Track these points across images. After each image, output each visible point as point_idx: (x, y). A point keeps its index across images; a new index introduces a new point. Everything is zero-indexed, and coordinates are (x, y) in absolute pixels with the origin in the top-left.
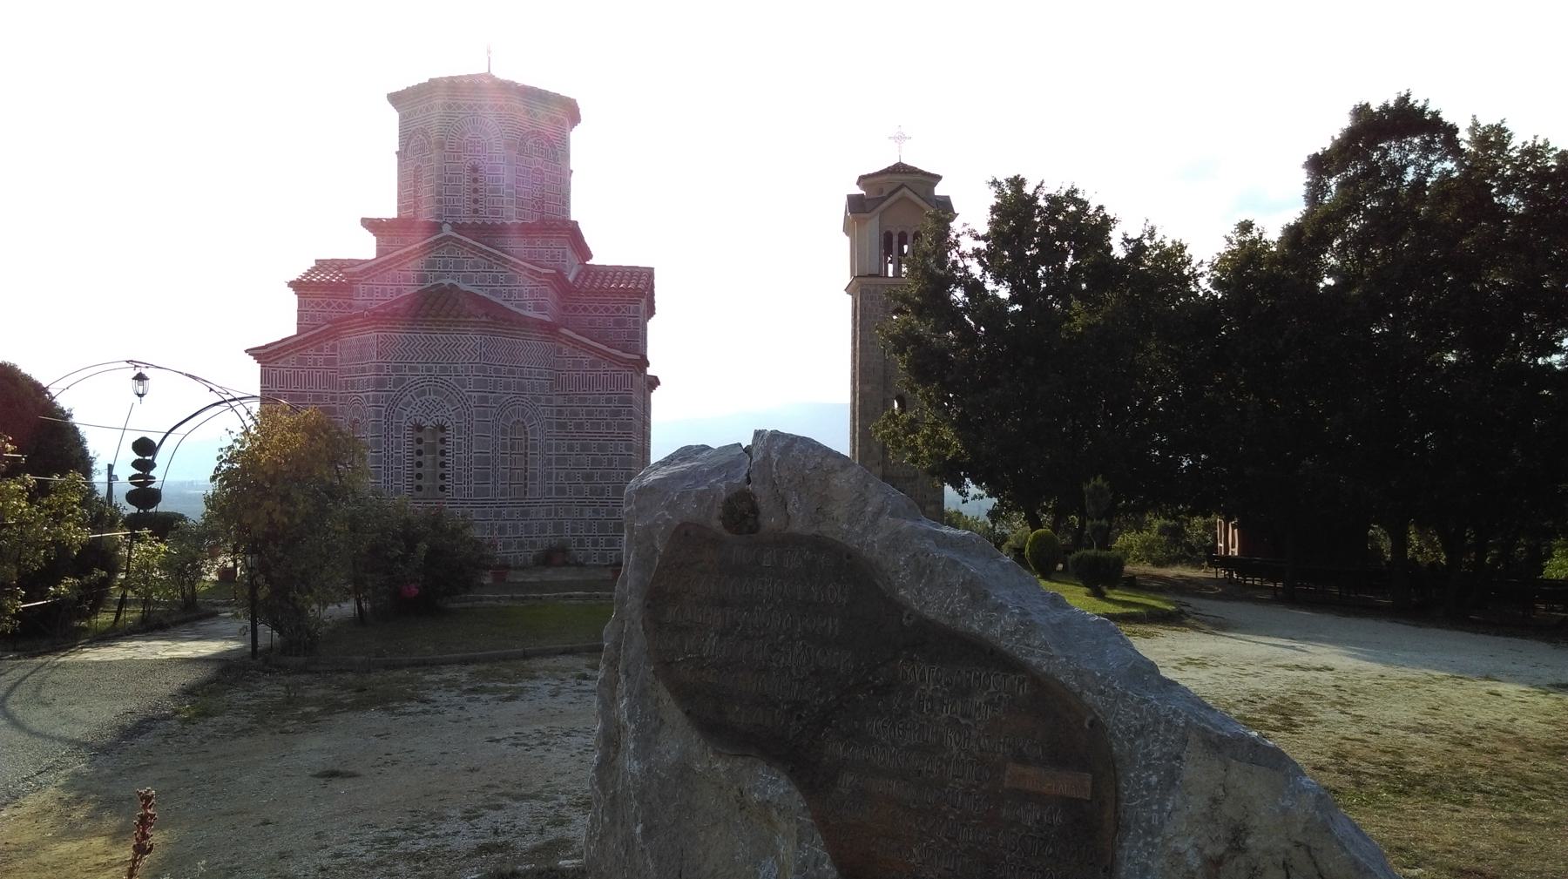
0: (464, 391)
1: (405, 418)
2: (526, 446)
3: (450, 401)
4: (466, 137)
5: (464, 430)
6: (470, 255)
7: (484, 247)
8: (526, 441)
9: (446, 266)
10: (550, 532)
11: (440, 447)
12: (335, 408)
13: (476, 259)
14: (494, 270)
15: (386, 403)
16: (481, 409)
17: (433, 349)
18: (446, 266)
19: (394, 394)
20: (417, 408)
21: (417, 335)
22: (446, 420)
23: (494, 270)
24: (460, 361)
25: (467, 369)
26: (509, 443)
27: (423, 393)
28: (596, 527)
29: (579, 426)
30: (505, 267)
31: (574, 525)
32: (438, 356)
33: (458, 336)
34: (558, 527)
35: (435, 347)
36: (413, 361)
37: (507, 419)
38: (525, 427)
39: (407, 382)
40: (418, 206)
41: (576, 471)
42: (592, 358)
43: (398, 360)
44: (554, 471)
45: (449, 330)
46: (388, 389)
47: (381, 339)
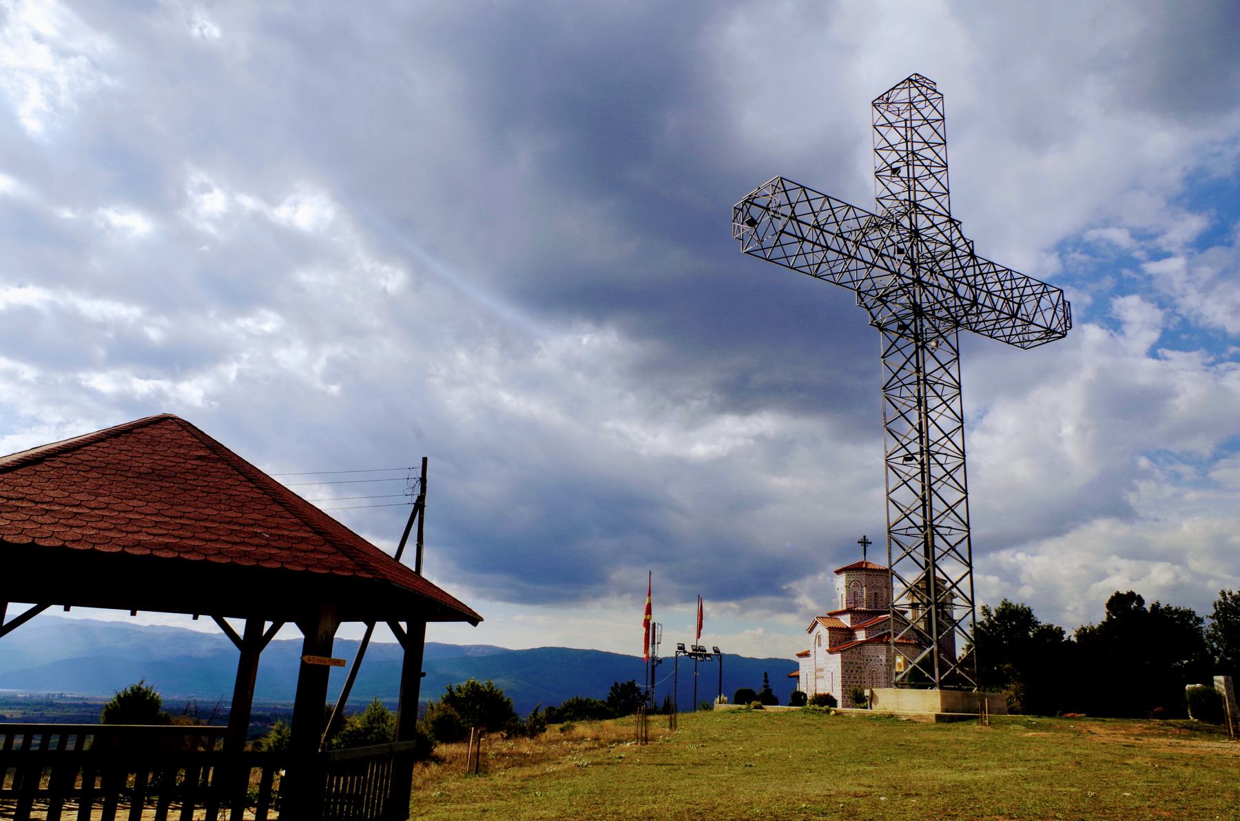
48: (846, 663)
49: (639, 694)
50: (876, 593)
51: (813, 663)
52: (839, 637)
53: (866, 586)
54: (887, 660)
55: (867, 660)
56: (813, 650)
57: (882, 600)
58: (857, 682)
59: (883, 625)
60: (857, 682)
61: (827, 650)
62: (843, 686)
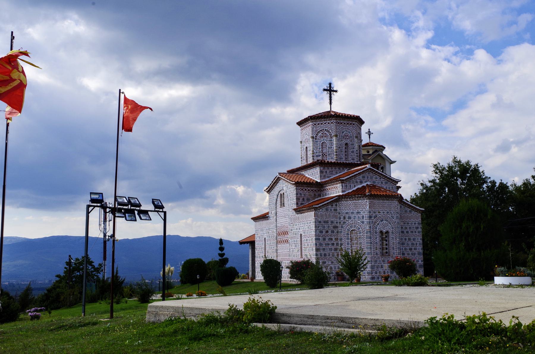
1: (378, 229)
3: (390, 223)
6: (374, 175)
9: (368, 178)
12: (337, 226)
13: (376, 176)
14: (381, 180)
15: (372, 223)
19: (374, 221)
20: (381, 226)
21: (380, 201)
23: (381, 180)
25: (394, 212)
27: (382, 221)
29: (407, 232)
30: (385, 179)
36: (379, 210)
39: (378, 217)
40: (323, 156)
42: (410, 209)
43: (375, 209)
44: (401, 247)
45: (389, 200)
46: (372, 219)
47: (370, 202)
48: (320, 222)
49: (93, 267)
50: (346, 144)
51: (273, 226)
52: (307, 193)
53: (336, 136)
54: (370, 217)
55: (344, 218)
56: (274, 212)
57: (353, 152)
58: (333, 244)
59: (361, 177)
60: (333, 244)
61: (295, 210)
62: (317, 250)
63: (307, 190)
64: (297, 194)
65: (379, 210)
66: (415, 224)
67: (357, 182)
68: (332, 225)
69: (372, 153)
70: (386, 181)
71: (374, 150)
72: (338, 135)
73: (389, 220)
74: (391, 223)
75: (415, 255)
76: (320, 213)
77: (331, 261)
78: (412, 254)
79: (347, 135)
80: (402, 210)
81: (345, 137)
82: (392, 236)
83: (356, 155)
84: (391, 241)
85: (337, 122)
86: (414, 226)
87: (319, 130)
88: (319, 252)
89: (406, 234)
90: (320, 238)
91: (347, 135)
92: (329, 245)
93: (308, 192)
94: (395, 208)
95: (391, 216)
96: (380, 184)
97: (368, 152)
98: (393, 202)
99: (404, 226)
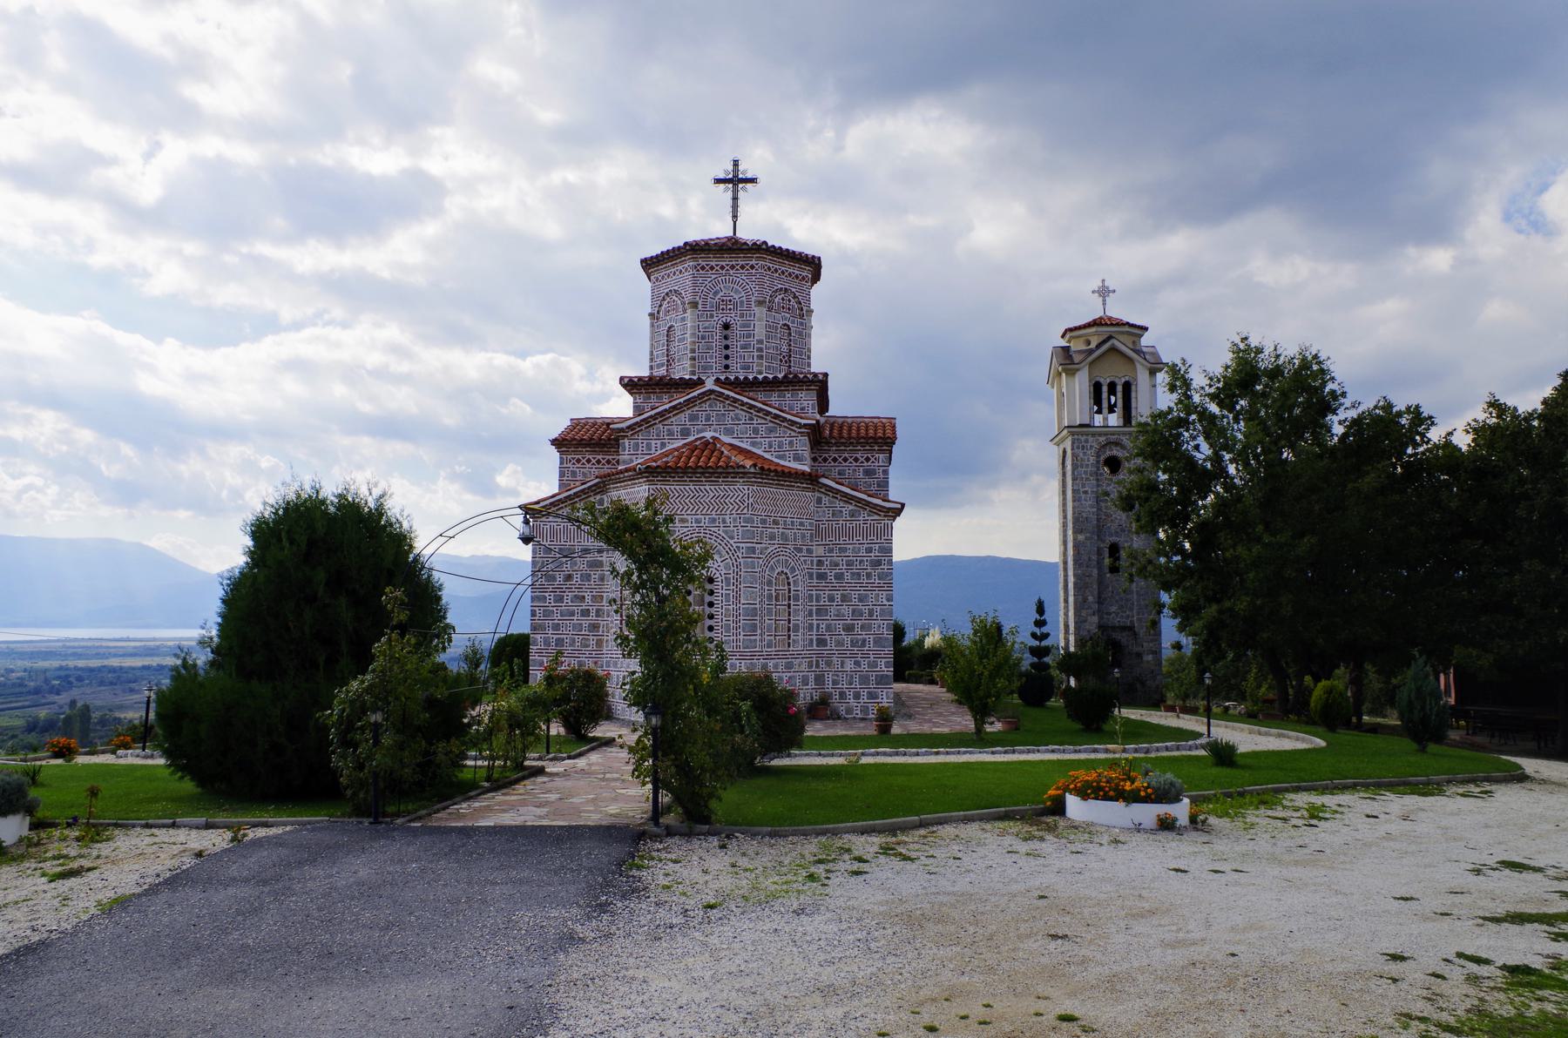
0: (732, 542)
2: (789, 597)
4: (719, 296)
5: (732, 581)
6: (731, 408)
7: (745, 400)
8: (789, 592)
9: (708, 419)
10: (812, 684)
11: (708, 599)
12: (602, 561)
13: (737, 411)
14: (755, 422)
16: (750, 560)
17: (702, 501)
18: (708, 419)
21: (687, 488)
22: (714, 571)
24: (728, 512)
25: (735, 520)
26: (774, 594)
28: (857, 680)
29: (839, 577)
30: (766, 419)
31: (836, 678)
32: (707, 507)
33: (726, 487)
34: (819, 680)
35: (704, 498)
36: (683, 513)
37: (772, 569)
38: (788, 578)
40: (671, 365)
41: (838, 622)
42: (851, 507)
47: (652, 491)
50: (726, 326)
58: (586, 613)
59: (683, 417)
60: (586, 613)
63: (594, 461)
64: (562, 474)
65: (683, 513)
66: (869, 550)
67: (670, 433)
68: (585, 559)
69: (1097, 346)
70: (771, 425)
71: (1105, 337)
72: (700, 302)
73: (716, 544)
74: (724, 553)
75: (863, 644)
76: (548, 527)
77: (577, 659)
78: (852, 641)
79: (728, 298)
80: (824, 511)
81: (721, 307)
82: (724, 592)
83: (756, 354)
84: (720, 606)
85: (699, 265)
86: (865, 559)
87: (662, 295)
88: (542, 636)
89: (833, 581)
90: (547, 594)
91: (728, 298)
92: (574, 615)
93: (597, 466)
94: (740, 507)
95: (723, 531)
96: (748, 435)
97: (1089, 343)
98: (731, 487)
99: (829, 559)
